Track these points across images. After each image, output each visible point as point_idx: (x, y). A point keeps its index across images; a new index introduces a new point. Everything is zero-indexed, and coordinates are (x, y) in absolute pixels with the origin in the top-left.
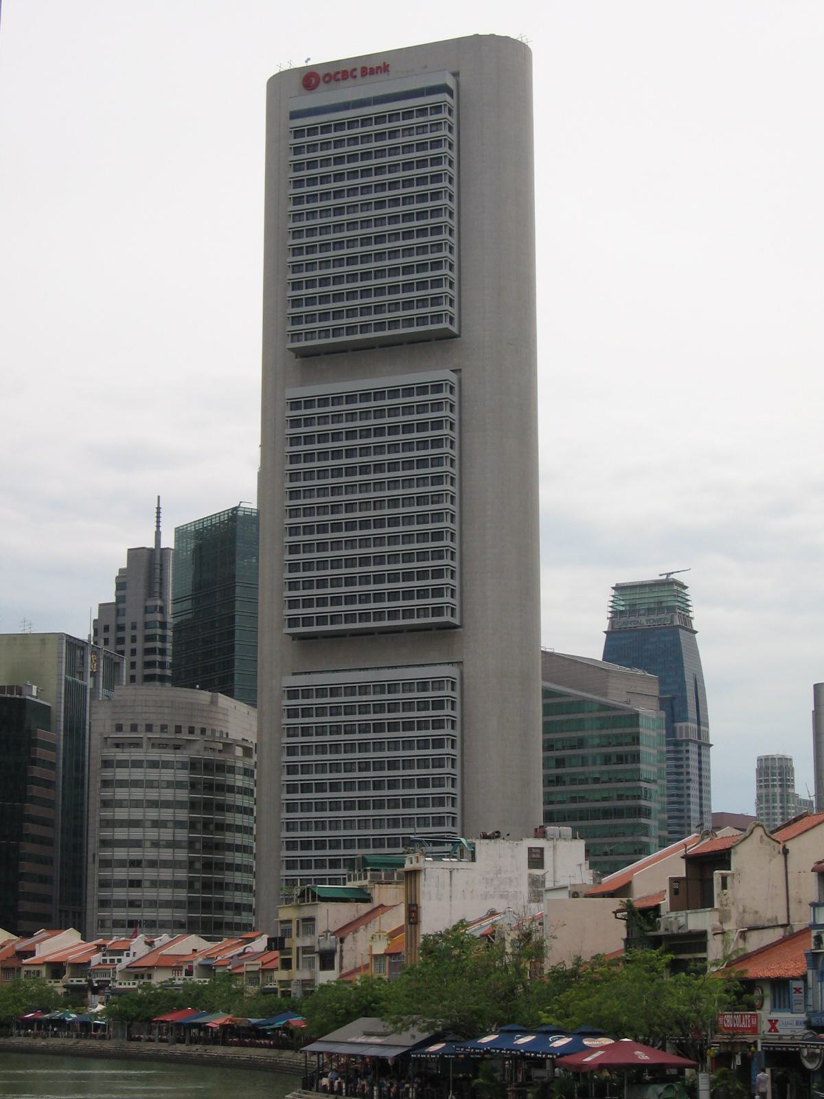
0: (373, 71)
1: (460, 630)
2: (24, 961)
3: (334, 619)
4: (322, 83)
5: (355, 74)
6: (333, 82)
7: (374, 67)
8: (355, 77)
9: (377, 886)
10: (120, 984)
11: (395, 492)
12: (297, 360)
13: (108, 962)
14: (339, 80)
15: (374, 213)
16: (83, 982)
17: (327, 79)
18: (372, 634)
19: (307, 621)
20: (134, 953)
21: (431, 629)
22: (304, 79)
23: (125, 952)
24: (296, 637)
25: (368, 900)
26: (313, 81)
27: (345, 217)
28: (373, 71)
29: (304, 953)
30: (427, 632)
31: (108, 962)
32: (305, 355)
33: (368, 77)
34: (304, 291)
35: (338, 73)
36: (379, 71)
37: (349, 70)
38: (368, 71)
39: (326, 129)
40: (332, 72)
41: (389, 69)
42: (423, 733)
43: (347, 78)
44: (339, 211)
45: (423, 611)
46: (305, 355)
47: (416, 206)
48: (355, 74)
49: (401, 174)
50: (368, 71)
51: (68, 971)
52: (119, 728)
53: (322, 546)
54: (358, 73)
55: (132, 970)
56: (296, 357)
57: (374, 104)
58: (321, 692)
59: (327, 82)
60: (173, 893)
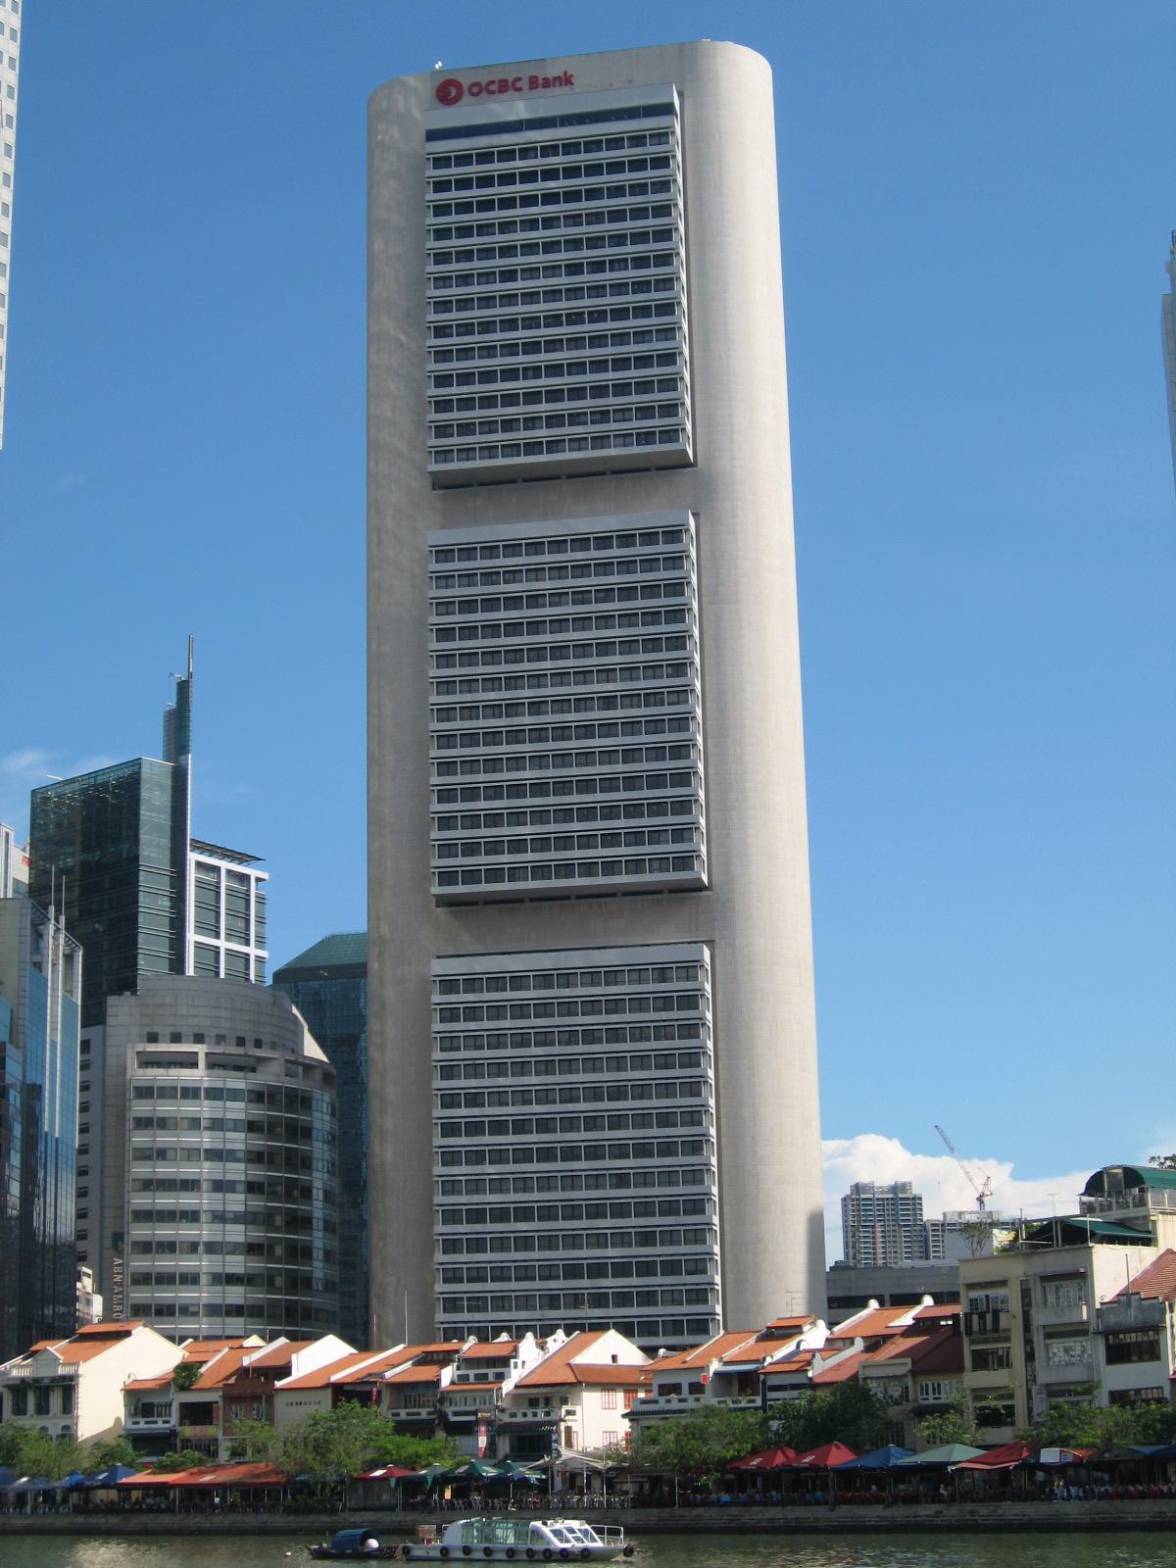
0: (547, 83)
1: (709, 893)
2: (279, 1384)
3: (515, 873)
4: (466, 96)
5: (519, 84)
6: (484, 94)
7: (550, 77)
8: (520, 89)
9: (1160, 1216)
10: (514, 1415)
11: (610, 687)
12: (435, 492)
13: (472, 1379)
14: (493, 92)
15: (563, 281)
16: (424, 1413)
17: (475, 90)
18: (567, 898)
19: (471, 876)
20: (524, 1362)
21: (660, 892)
22: (441, 85)
23: (512, 1361)
24: (445, 902)
25: (1148, 1241)
26: (453, 91)
27: (519, 284)
28: (547, 83)
29: (1049, 1335)
30: (657, 896)
31: (472, 1379)
32: (444, 484)
33: (540, 91)
34: (455, 390)
35: (492, 82)
36: (557, 83)
37: (510, 80)
38: (540, 82)
39: (485, 157)
40: (484, 81)
41: (573, 80)
42: (665, 1044)
43: (506, 91)
44: (509, 275)
45: (661, 863)
46: (444, 484)
47: (632, 274)
48: (519, 84)
49: (607, 228)
50: (540, 82)
51: (386, 1398)
52: (153, 1038)
53: (493, 764)
54: (524, 84)
55: (521, 1391)
56: (434, 489)
57: (562, 125)
58: (496, 982)
59: (472, 94)
60: (224, 1298)
